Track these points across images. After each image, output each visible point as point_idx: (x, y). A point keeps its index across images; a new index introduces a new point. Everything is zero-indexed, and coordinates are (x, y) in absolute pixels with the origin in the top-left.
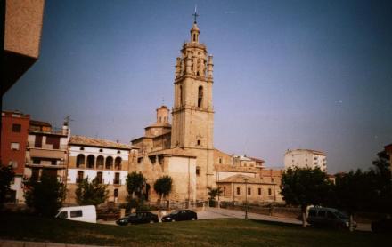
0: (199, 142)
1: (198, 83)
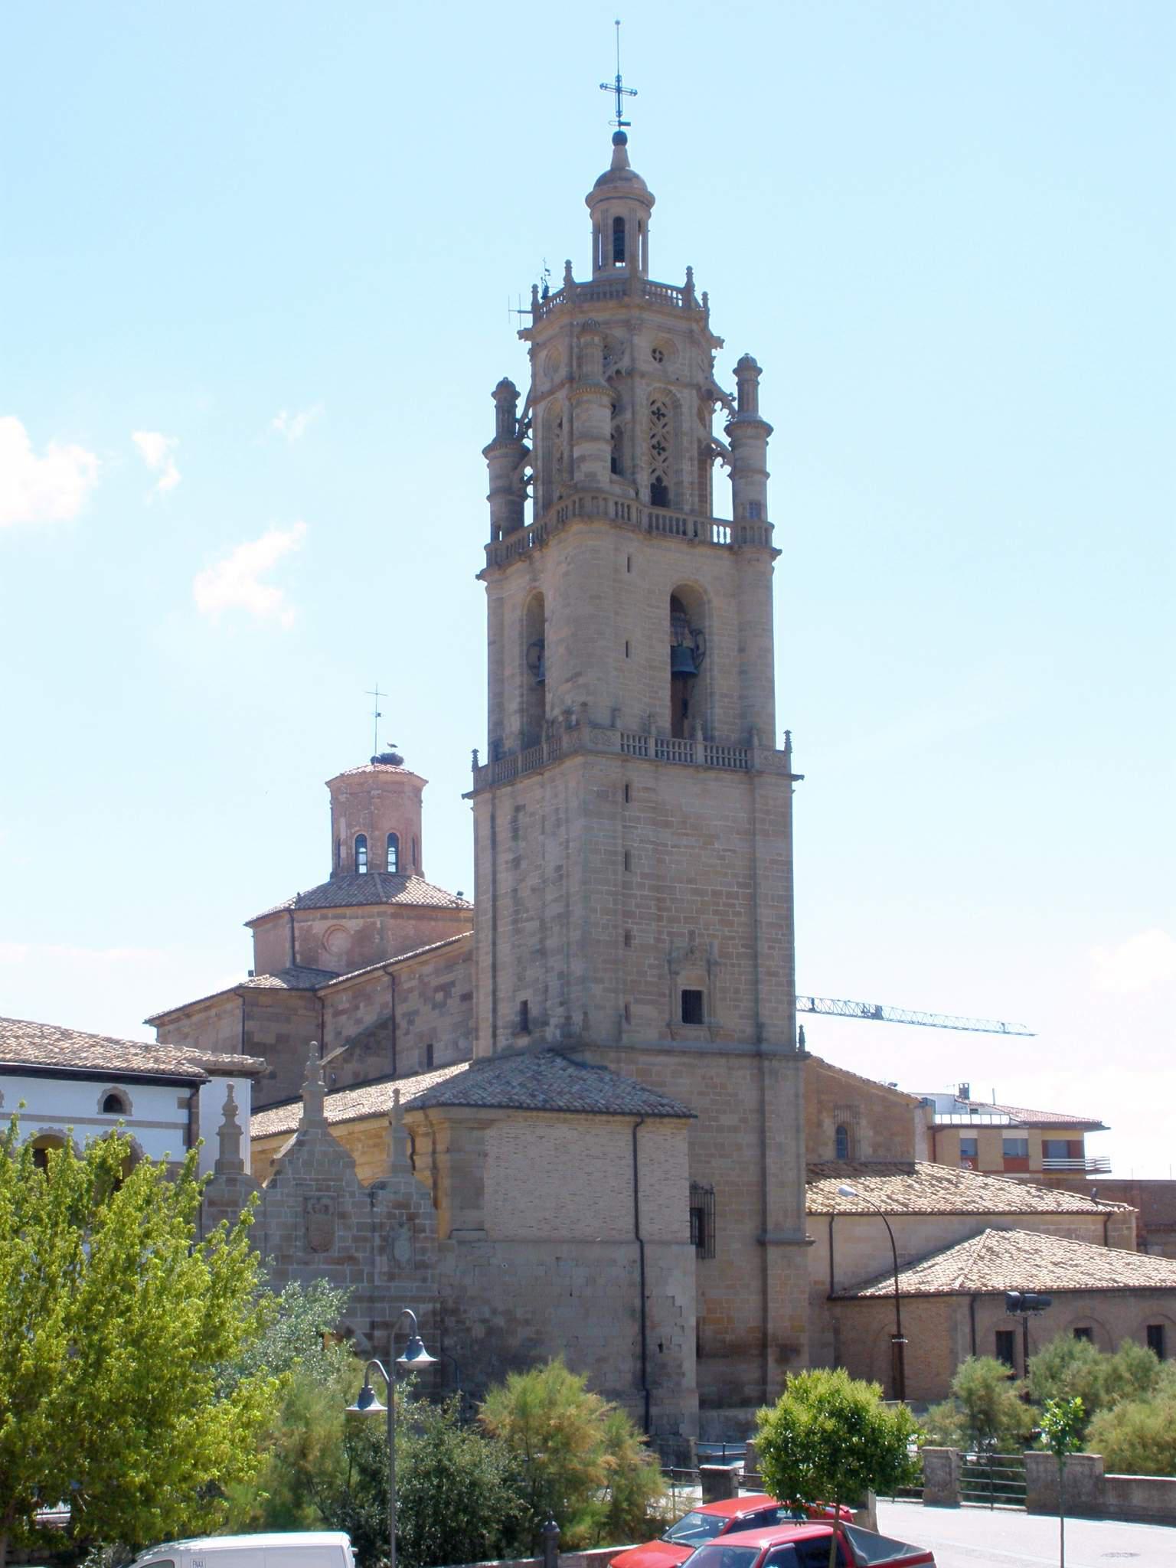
0: (692, 1006)
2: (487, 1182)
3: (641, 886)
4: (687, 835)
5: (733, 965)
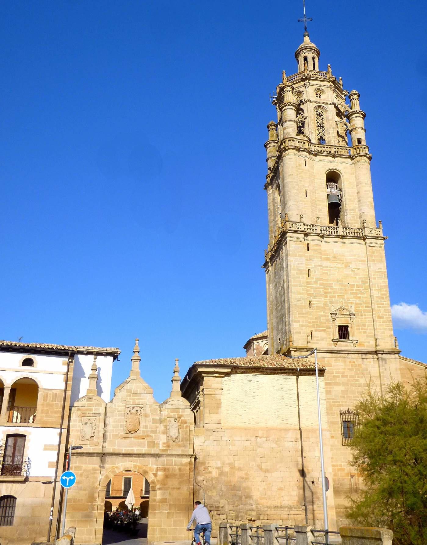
0: (344, 332)
1: (324, 165)
2: (223, 401)
3: (315, 283)
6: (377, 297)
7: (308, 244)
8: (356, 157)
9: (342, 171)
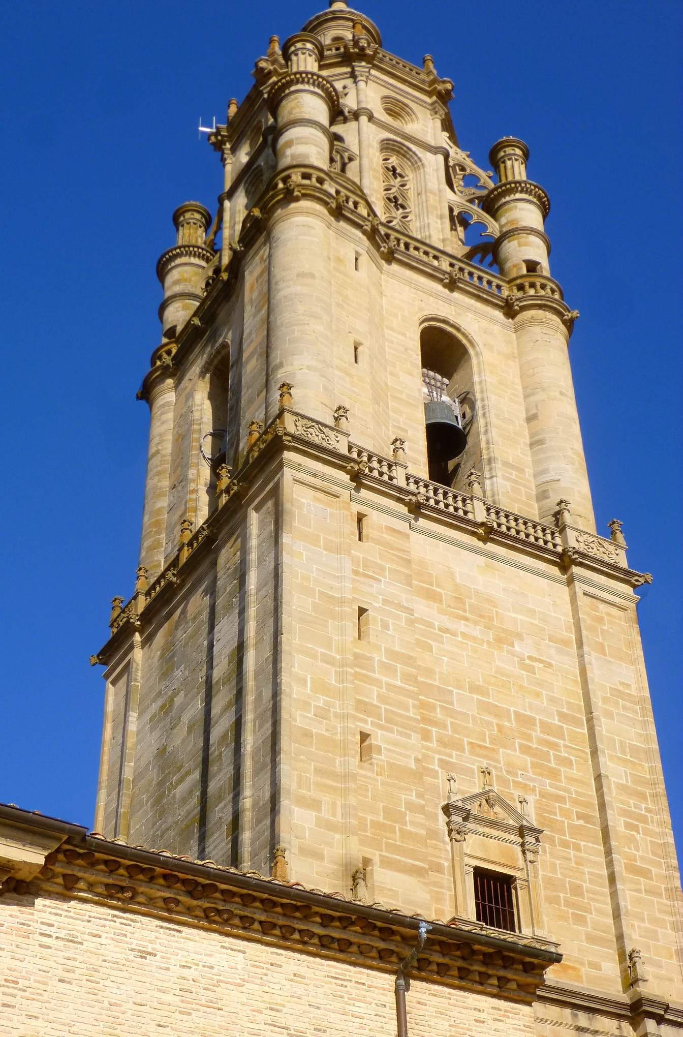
3: (388, 669)
4: (466, 619)
5: (565, 844)
6: (623, 788)
7: (360, 518)
8: (523, 309)
9: (476, 338)
